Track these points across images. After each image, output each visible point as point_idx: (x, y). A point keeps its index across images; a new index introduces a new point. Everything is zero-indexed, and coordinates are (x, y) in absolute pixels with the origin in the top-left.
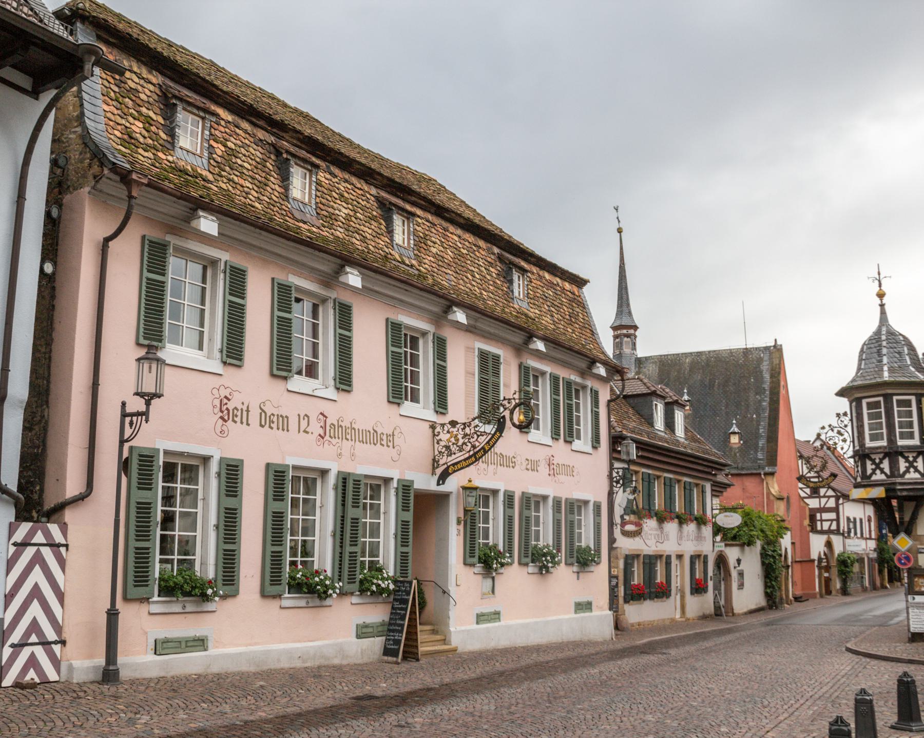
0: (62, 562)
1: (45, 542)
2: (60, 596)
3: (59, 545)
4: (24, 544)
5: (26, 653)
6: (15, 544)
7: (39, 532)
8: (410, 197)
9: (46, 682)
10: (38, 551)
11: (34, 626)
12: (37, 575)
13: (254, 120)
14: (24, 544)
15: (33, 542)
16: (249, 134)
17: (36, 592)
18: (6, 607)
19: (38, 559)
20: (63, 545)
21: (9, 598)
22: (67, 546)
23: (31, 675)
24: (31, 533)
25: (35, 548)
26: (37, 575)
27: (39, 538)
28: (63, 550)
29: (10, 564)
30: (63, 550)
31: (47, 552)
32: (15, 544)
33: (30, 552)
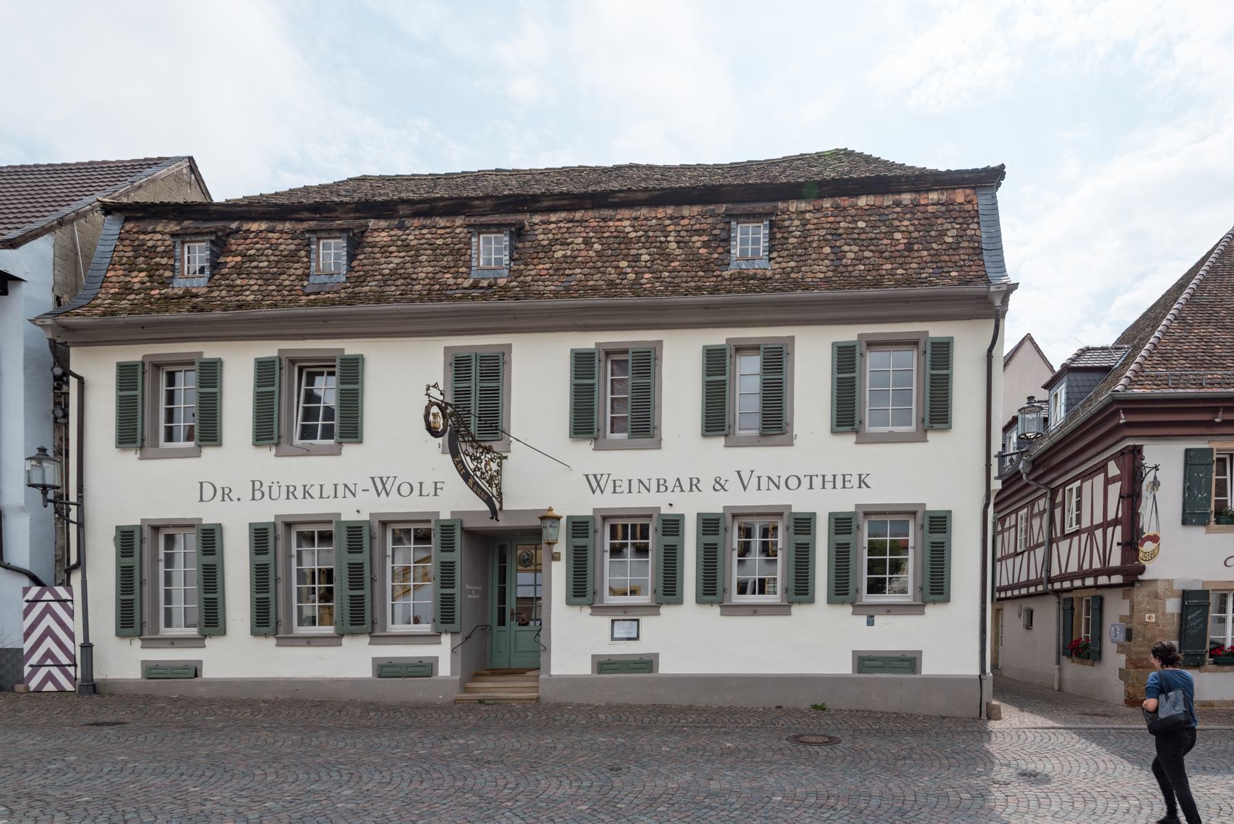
0: (71, 614)
1: (53, 599)
2: (71, 636)
3: (66, 601)
4: (35, 601)
5: (43, 672)
6: (27, 601)
7: (48, 593)
8: (538, 205)
9: (62, 691)
10: (48, 605)
11: (49, 654)
12: (48, 621)
13: (298, 216)
14: (35, 601)
15: (43, 599)
16: (286, 232)
17: (48, 632)
18: (25, 640)
19: (48, 610)
20: (69, 600)
21: (27, 635)
22: (72, 601)
23: (50, 687)
24: (40, 594)
25: (46, 603)
26: (48, 621)
27: (48, 596)
28: (69, 603)
29: (26, 613)
30: (69, 603)
31: (56, 606)
32: (27, 601)
33: (40, 607)
